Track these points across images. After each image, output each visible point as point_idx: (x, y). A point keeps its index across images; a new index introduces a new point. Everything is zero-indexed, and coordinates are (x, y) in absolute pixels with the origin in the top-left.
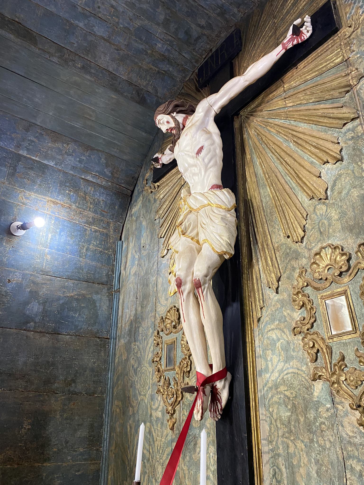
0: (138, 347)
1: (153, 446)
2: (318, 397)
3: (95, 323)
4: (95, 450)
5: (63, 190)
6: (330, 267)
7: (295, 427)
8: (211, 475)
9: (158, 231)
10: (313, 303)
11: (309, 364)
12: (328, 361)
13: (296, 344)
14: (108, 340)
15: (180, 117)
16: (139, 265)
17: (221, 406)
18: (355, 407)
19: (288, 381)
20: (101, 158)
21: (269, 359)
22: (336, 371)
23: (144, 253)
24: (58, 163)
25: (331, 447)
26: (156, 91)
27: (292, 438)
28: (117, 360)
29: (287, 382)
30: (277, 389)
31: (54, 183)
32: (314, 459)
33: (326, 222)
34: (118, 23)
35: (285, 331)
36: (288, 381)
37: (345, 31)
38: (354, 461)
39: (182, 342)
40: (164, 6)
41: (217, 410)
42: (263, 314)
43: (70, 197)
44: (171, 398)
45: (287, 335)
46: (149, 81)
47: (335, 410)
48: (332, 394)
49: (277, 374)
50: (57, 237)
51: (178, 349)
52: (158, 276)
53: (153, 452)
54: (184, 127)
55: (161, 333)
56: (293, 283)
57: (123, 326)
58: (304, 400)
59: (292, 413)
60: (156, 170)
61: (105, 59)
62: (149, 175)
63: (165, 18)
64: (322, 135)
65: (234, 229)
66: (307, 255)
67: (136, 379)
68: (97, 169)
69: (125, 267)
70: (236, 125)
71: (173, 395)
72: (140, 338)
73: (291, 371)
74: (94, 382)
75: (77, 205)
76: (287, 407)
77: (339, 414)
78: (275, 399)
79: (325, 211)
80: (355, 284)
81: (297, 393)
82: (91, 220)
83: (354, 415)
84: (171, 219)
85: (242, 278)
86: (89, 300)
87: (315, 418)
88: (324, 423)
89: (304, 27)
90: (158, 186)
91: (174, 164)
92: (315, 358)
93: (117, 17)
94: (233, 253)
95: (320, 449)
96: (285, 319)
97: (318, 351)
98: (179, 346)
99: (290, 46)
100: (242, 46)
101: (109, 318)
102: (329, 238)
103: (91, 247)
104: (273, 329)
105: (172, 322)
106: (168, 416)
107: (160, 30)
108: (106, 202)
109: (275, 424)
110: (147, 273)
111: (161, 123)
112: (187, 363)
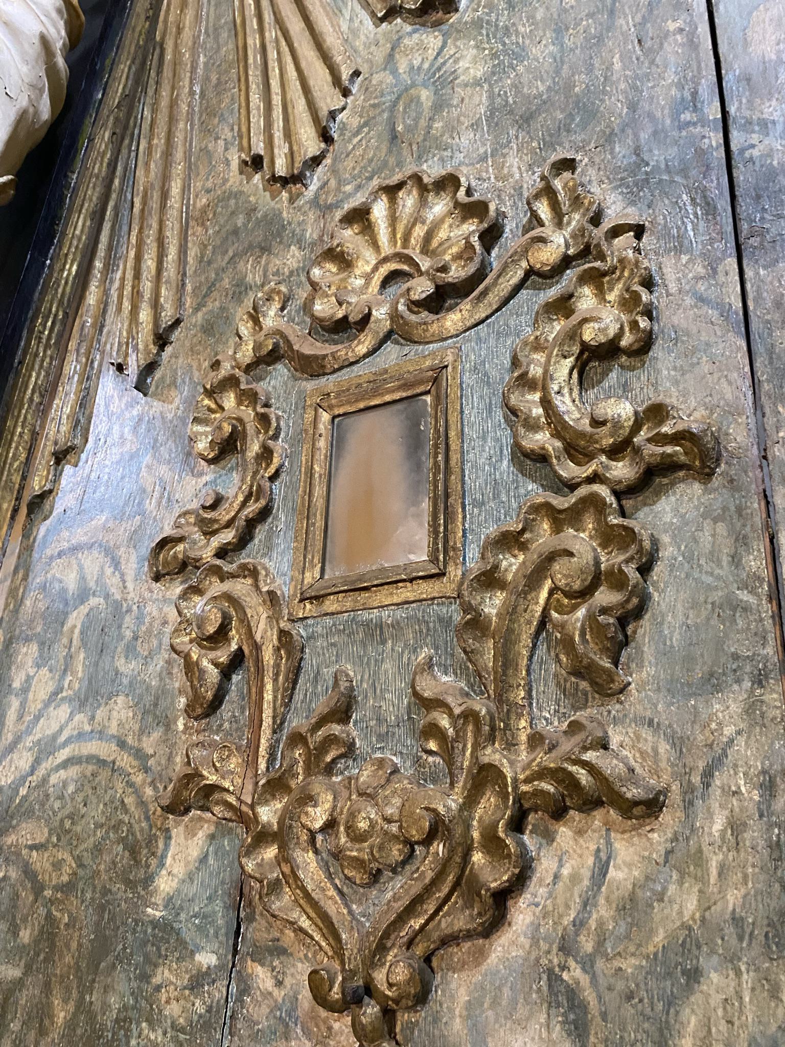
10: (278, 429)
19: (61, 797)
21: (16, 684)
22: (290, 772)
29: (57, 805)
33: (426, 95)
36: (61, 797)
42: (63, 481)
45: (122, 575)
47: (233, 988)
58: (102, 908)
76: (16, 934)
79: (431, 54)
80: (492, 342)
81: (81, 865)
85: (31, 331)
92: (210, 695)
97: (237, 659)
104: (75, 549)
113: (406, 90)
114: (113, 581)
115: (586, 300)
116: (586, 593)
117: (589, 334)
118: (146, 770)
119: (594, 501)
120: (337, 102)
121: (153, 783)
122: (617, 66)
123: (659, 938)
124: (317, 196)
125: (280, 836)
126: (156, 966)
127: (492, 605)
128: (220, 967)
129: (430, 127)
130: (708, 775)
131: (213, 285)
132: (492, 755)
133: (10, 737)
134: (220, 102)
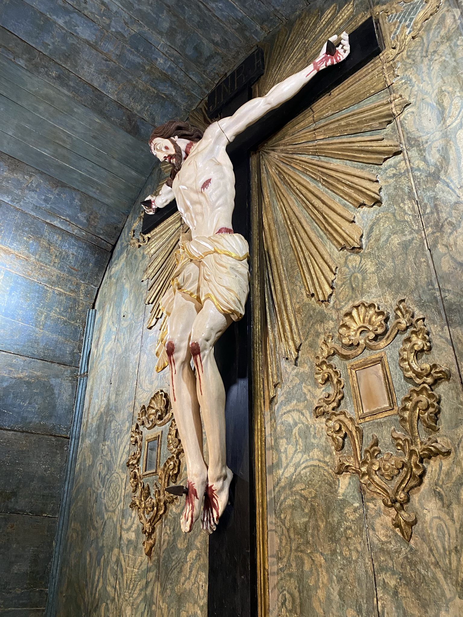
0: (108, 447)
1: (121, 581)
2: (343, 495)
3: (51, 416)
4: (38, 591)
5: (20, 235)
6: (363, 329)
7: (313, 536)
8: (199, 612)
9: (145, 295)
10: (341, 375)
11: (334, 453)
12: (357, 447)
13: (317, 429)
14: (68, 440)
15: (183, 143)
16: (117, 340)
17: (218, 514)
18: (389, 503)
20: (74, 199)
21: (282, 450)
22: (367, 459)
23: (125, 324)
24: (16, 199)
25: (358, 558)
26: (153, 119)
27: (309, 551)
28: (78, 467)
29: (305, 478)
30: (291, 488)
31: (8, 225)
32: (336, 577)
33: (359, 276)
34: (109, 25)
36: (306, 476)
37: (388, 53)
38: (388, 575)
39: (170, 436)
40: (170, 11)
41: (212, 519)
42: (279, 393)
43: (28, 247)
44: (149, 512)
45: (306, 418)
46: (145, 106)
47: (365, 509)
48: (361, 490)
49: (291, 469)
50: (6, 297)
51: (162, 446)
52: (142, 353)
53: (120, 588)
54: (187, 155)
55: (141, 428)
56: (316, 351)
57: (90, 420)
59: (310, 518)
60: (147, 216)
61: (88, 71)
62: (137, 224)
63: (170, 27)
64: (358, 172)
65: (245, 283)
66: (335, 317)
67: (104, 491)
68: (69, 212)
69: (98, 344)
70: (253, 161)
71: (153, 507)
72: (112, 435)
73: (310, 463)
74: (43, 496)
75: (37, 257)
76: (303, 511)
77: (370, 515)
78: (289, 502)
79: (358, 262)
80: (393, 350)
82: (54, 278)
83: (388, 515)
84: (164, 279)
85: (254, 348)
86: (44, 384)
87: (339, 523)
88: (350, 528)
89: (341, 46)
90: (149, 239)
91: (172, 208)
92: (341, 445)
93: (110, 18)
94: (243, 313)
95: (345, 562)
97: (346, 435)
98: (165, 442)
99: (323, 67)
100: (264, 69)
101: (70, 411)
102: (362, 295)
103: (52, 314)
104: (289, 412)
105: (157, 411)
106: (144, 537)
107: (163, 41)
108: (77, 257)
109: (287, 534)
110: (126, 350)
111: (157, 149)
112: (174, 464)
113: (353, 274)
114: (303, 419)
115: (414, 338)
116: (427, 409)
117: (416, 347)
118: (328, 466)
119: (424, 388)
120: (333, 277)
121: (331, 469)
122: (410, 271)
123: (454, 478)
124: (333, 306)
125: (368, 473)
127: (406, 415)
128: (361, 505)
129: (362, 286)
130: (458, 445)
131: (308, 332)
132: (412, 448)
133: (285, 465)
134: (294, 273)
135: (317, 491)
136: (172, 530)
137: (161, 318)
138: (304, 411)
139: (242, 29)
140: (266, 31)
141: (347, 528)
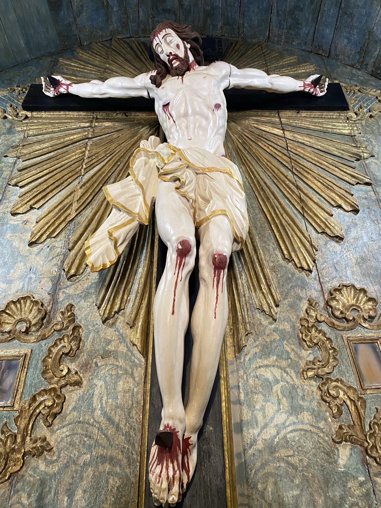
2: (345, 466)
6: (354, 308)
26: (80, 13)
29: (293, 443)
35: (289, 371)
42: (249, 343)
45: (291, 377)
48: (365, 463)
49: (273, 432)
59: (302, 490)
73: (300, 426)
96: (288, 355)
104: (267, 366)
111: (165, 40)
114: (288, 378)
121: (327, 436)
126: (347, 483)
135: (310, 460)
136: (33, 499)
137: (38, 209)
138: (288, 369)
139: (209, 14)
140: (222, 32)
141: (352, 504)
